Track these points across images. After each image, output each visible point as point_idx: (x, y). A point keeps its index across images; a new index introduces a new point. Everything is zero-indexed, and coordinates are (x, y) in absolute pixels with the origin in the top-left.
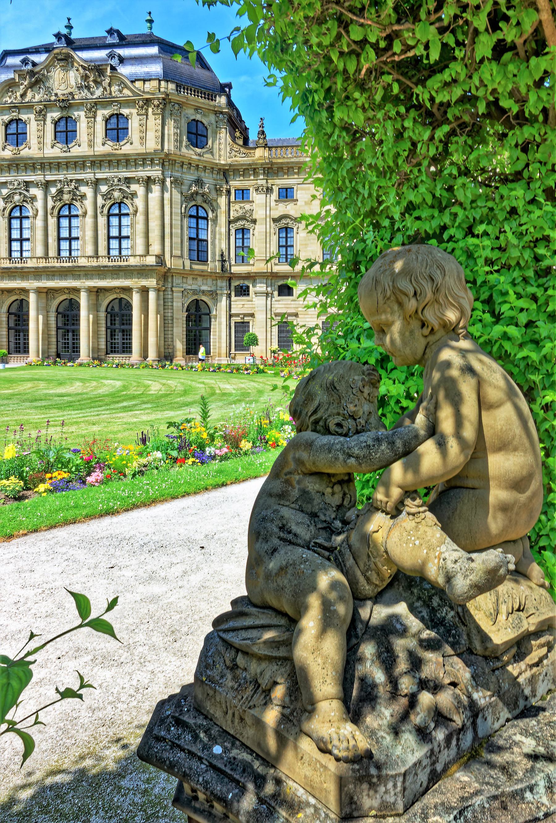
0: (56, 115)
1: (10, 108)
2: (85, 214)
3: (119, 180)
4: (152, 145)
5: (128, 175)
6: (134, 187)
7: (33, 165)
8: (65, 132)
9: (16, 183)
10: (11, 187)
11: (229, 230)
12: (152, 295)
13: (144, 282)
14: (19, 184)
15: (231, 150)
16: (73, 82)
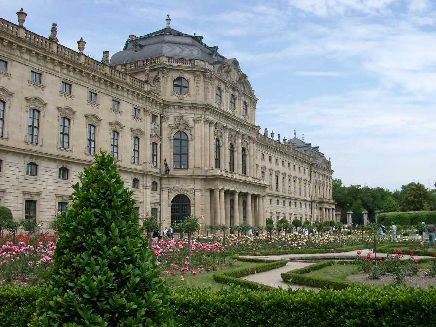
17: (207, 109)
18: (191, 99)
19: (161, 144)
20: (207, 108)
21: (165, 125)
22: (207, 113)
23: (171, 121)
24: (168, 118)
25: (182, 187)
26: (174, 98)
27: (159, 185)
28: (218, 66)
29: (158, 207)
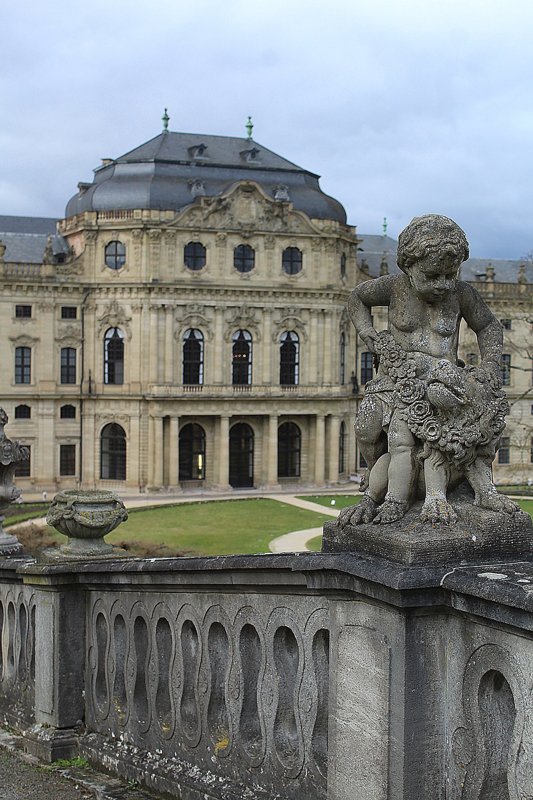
0: (236, 241)
1: (191, 231)
2: (259, 340)
3: (295, 311)
4: (324, 279)
5: (303, 306)
6: (305, 316)
7: (213, 290)
8: (244, 259)
9: (196, 307)
10: (190, 311)
11: (357, 353)
12: (335, 424)
13: (330, 412)
14: (198, 308)
15: (360, 277)
16: (254, 213)
17: (150, 290)
18: (129, 274)
19: (83, 348)
20: (152, 287)
21: (90, 318)
22: (153, 295)
23: (100, 314)
24: (96, 309)
25: (114, 412)
26: (106, 275)
27: (78, 410)
28: (188, 208)
29: (76, 442)
